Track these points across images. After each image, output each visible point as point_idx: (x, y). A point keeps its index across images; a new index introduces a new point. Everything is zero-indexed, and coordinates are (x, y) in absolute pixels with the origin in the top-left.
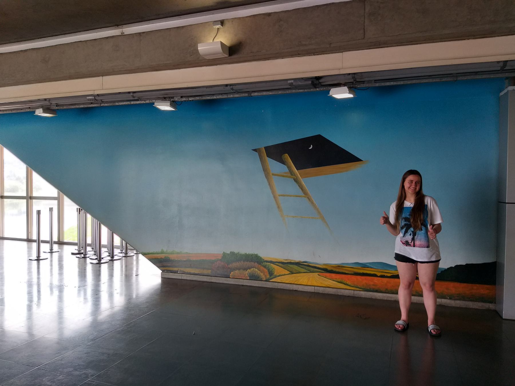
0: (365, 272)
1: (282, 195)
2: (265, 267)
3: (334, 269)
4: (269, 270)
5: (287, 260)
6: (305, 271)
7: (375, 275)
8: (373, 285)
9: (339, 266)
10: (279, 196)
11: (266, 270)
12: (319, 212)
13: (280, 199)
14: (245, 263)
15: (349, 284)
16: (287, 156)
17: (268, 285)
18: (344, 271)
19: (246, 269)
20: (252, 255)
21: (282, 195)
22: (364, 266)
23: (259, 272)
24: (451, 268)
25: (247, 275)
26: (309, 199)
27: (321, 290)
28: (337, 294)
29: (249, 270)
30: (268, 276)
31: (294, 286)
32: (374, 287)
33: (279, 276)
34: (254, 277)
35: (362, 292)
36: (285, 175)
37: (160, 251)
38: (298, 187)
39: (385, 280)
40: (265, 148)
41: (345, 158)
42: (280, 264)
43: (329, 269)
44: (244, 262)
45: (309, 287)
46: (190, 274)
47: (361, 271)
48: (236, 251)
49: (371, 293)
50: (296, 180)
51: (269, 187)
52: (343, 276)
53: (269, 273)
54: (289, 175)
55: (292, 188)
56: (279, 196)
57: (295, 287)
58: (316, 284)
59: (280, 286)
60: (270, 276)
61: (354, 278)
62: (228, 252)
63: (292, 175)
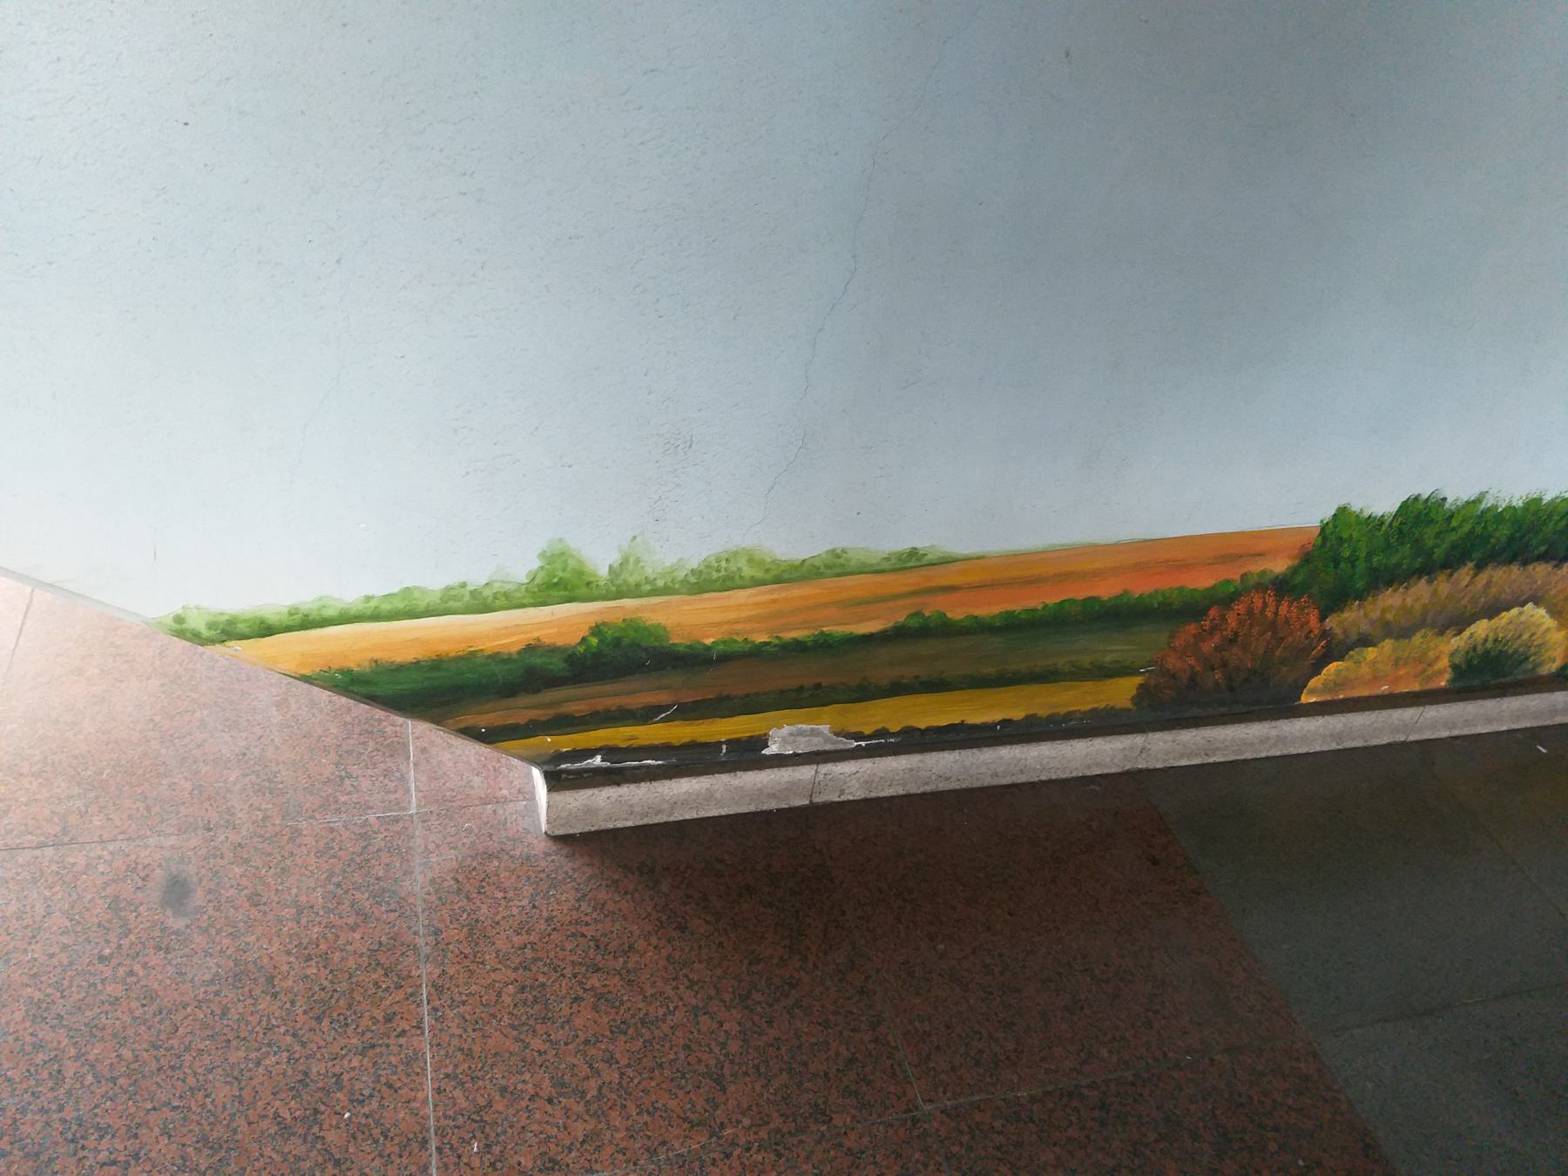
14: (1483, 578)
19: (1460, 623)
23: (1549, 622)
25: (1444, 663)
29: (1481, 628)
37: (521, 567)
48: (1457, 491)
62: (1382, 502)
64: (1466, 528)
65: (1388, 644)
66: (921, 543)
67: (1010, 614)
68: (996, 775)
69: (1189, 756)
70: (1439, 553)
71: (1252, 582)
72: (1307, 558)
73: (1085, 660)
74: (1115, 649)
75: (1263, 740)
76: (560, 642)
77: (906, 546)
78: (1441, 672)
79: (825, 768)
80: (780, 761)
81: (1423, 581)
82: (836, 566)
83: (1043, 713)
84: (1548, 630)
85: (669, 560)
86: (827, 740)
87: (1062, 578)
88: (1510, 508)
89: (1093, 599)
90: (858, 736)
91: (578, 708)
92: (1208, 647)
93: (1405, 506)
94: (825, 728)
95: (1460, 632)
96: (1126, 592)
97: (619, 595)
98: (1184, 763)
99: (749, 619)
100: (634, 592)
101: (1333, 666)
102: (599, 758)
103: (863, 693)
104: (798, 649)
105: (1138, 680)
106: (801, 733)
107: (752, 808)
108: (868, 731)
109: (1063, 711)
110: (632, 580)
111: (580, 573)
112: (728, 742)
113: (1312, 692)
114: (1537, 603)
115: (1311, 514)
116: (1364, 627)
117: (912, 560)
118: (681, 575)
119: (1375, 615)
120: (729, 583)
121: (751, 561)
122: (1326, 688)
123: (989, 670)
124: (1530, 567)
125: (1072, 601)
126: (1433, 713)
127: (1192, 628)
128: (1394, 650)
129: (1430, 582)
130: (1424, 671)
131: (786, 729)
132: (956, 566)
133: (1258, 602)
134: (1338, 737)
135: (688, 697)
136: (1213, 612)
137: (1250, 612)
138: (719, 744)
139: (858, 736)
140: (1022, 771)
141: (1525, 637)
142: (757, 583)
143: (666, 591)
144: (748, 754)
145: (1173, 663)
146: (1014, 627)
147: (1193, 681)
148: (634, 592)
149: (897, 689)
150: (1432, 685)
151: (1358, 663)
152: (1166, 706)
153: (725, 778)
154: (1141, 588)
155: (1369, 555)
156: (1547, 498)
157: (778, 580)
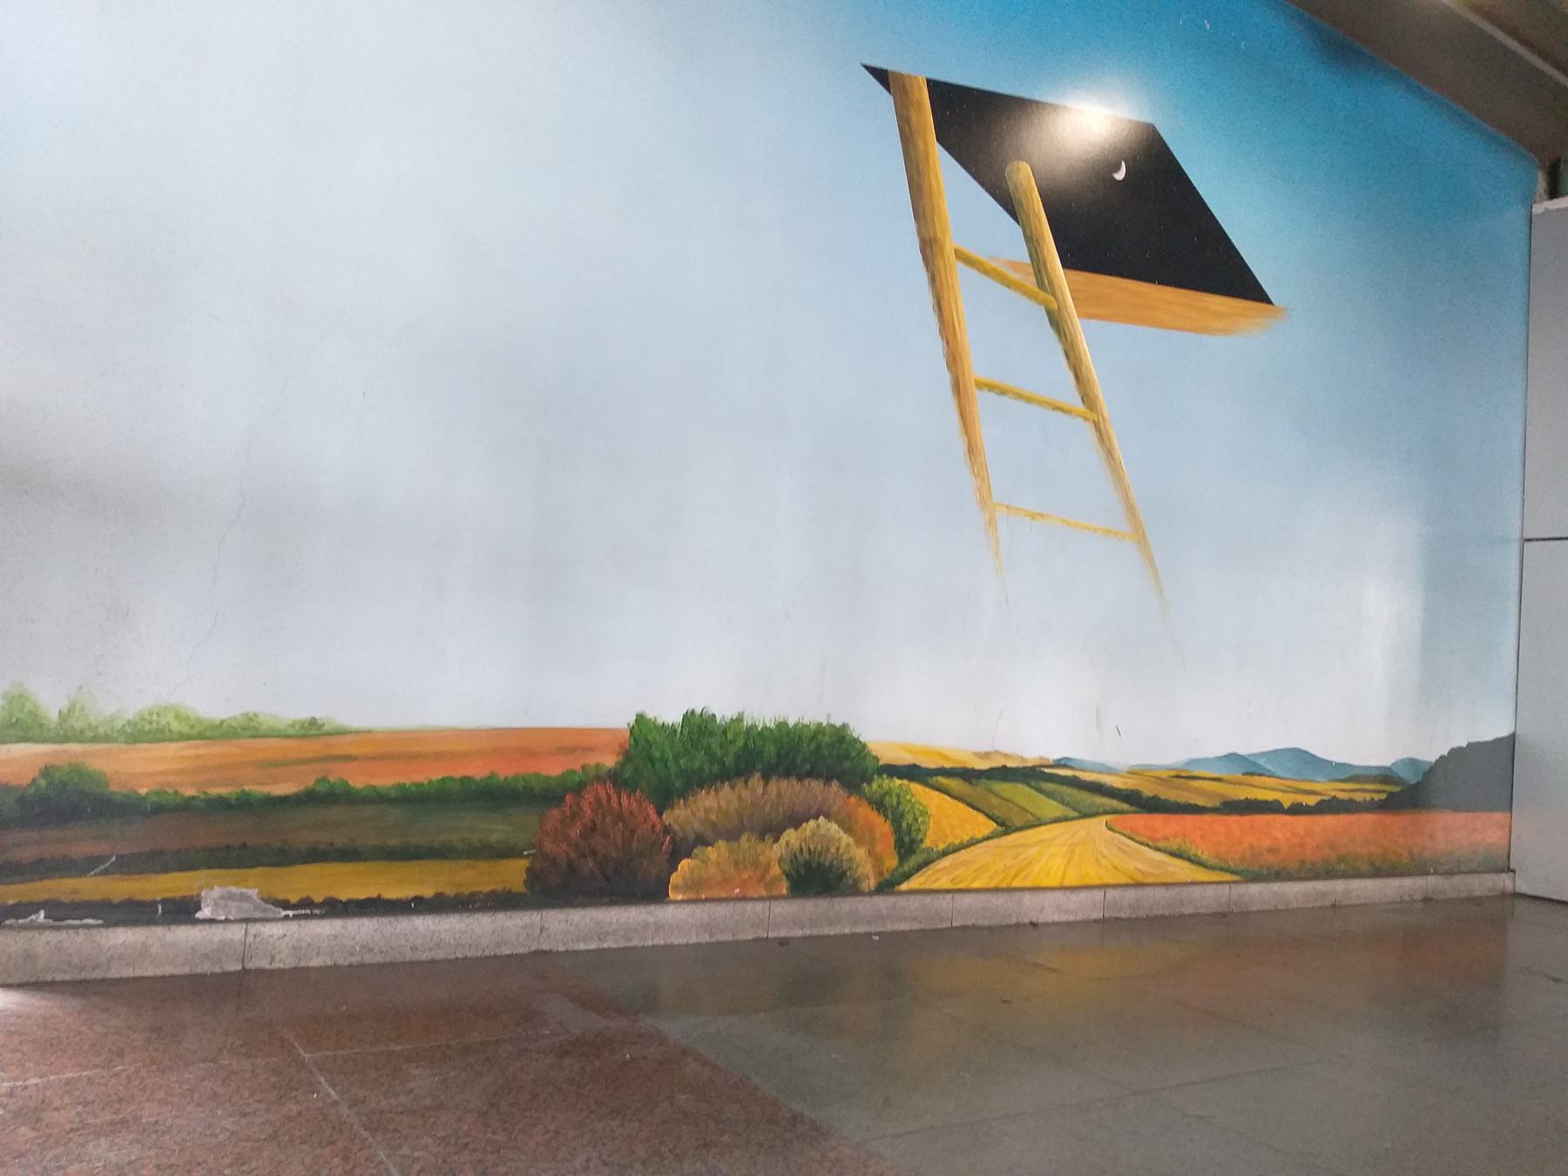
1: (991, 387)
2: (879, 805)
4: (897, 820)
8: (1270, 851)
9: (1181, 776)
10: (981, 385)
11: (883, 827)
12: (1131, 509)
13: (983, 402)
14: (773, 786)
15: (1204, 856)
19: (772, 830)
20: (820, 730)
21: (991, 387)
22: (1250, 767)
23: (846, 839)
24: (1442, 757)
25: (776, 870)
29: (790, 836)
30: (892, 862)
32: (1270, 858)
33: (945, 853)
34: (816, 877)
35: (1254, 889)
36: (1014, 275)
39: (1301, 821)
40: (935, 87)
41: (1228, 276)
42: (954, 784)
43: (1148, 791)
44: (766, 778)
45: (1083, 896)
46: (334, 908)
48: (723, 711)
49: (1276, 887)
50: (1057, 322)
52: (1190, 820)
53: (900, 844)
54: (1030, 282)
56: (981, 385)
58: (1094, 875)
59: (965, 910)
60: (903, 858)
63: (1041, 285)
64: (740, 743)
65: (721, 843)
66: (319, 715)
67: (400, 787)
68: (414, 949)
69: (586, 939)
71: (592, 774)
72: (628, 756)
73: (475, 838)
74: (496, 829)
75: (646, 926)
76: (14, 782)
77: (304, 714)
78: (775, 880)
79: (254, 929)
80: (211, 921)
82: (247, 729)
83: (450, 891)
84: (848, 845)
85: (109, 710)
86: (256, 908)
87: (439, 756)
88: (765, 728)
89: (466, 779)
90: (286, 905)
91: (27, 854)
92: (575, 832)
93: (689, 717)
94: (253, 893)
95: (776, 840)
96: (493, 775)
97: (65, 739)
98: (582, 946)
99: (178, 772)
100: (78, 737)
101: (685, 864)
102: (42, 914)
103: (285, 857)
104: (221, 806)
106: (231, 897)
107: (187, 970)
108: (294, 899)
109: (466, 891)
110: (79, 725)
111: (34, 715)
112: (164, 902)
113: (676, 888)
114: (827, 816)
115: (620, 719)
116: (697, 826)
117: (311, 730)
118: (119, 724)
119: (701, 814)
120: (159, 735)
121: (178, 716)
123: (394, 842)
124: (806, 782)
125: (451, 778)
127: (555, 813)
128: (730, 851)
129: (733, 787)
130: (763, 877)
131: (217, 891)
132: (349, 738)
133: (603, 795)
134: (708, 928)
135: (125, 849)
136: (568, 798)
137: (598, 800)
138: (154, 903)
140: (438, 946)
141: (833, 850)
142: (183, 737)
143: (107, 739)
144: (183, 911)
145: (549, 846)
146: (411, 799)
147: (572, 869)
148: (78, 737)
149: (316, 855)
150: (775, 893)
151: (704, 862)
152: (554, 886)
153: (159, 931)
154: (505, 772)
155: (676, 758)
156: (791, 723)
157: (201, 736)
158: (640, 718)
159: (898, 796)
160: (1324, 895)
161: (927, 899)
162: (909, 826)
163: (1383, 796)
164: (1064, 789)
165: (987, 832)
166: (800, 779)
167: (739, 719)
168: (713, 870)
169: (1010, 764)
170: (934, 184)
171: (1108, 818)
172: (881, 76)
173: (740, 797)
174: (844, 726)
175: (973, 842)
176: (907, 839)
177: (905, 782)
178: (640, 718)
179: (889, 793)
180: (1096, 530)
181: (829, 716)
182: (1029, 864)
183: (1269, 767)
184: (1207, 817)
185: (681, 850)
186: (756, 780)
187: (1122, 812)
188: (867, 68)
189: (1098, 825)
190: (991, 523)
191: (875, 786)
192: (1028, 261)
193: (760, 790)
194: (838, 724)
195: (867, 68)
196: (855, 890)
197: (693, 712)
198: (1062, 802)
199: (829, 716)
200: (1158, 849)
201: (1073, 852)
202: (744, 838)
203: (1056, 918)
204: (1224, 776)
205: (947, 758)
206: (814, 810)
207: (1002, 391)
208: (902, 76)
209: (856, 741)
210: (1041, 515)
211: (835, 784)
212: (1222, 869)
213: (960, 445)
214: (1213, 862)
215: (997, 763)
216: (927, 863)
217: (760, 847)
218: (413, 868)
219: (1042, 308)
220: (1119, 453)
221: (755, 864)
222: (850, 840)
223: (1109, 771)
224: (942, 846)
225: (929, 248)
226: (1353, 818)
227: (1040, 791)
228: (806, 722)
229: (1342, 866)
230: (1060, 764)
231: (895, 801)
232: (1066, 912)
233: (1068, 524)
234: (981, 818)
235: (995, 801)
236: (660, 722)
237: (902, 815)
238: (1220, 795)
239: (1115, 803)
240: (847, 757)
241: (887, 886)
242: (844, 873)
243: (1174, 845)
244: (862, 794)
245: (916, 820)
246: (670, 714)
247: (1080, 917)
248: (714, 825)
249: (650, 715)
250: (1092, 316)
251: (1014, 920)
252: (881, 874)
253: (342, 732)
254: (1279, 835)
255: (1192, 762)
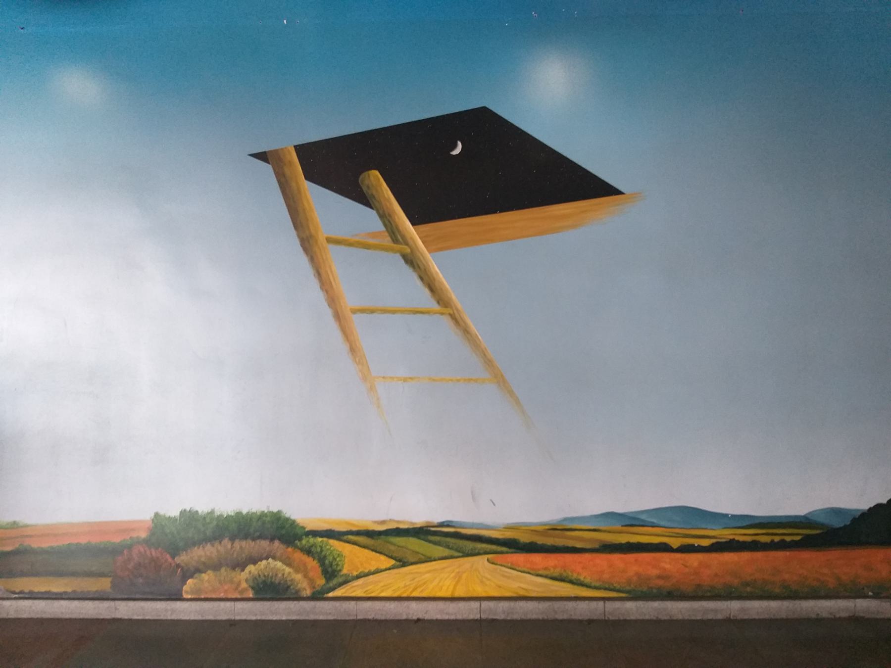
0: (634, 539)
1: (363, 311)
2: (308, 552)
3: (540, 540)
4: (322, 560)
5: (383, 522)
6: (447, 552)
7: (664, 548)
8: (659, 577)
9: (554, 529)
10: (354, 311)
11: (312, 563)
12: (489, 363)
13: (358, 322)
14: (237, 544)
15: (588, 580)
16: (375, 180)
17: (323, 611)
18: (570, 543)
19: (240, 565)
20: (263, 515)
21: (363, 311)
22: (632, 521)
23: (288, 570)
25: (244, 585)
26: (456, 319)
27: (500, 611)
28: (551, 616)
29: (251, 568)
30: (321, 582)
31: (414, 605)
32: (661, 583)
33: (358, 577)
34: (270, 590)
35: (630, 605)
36: (371, 241)
38: (419, 282)
39: (694, 559)
40: (299, 149)
43: (524, 538)
44: (232, 539)
45: (462, 605)
46: (33, 596)
47: (623, 539)
48: (202, 507)
49: (656, 604)
50: (411, 260)
51: (314, 283)
52: (569, 557)
54: (387, 241)
55: (397, 284)
56: (354, 311)
57: (415, 610)
58: (480, 591)
61: (602, 561)
62: (174, 513)
63: (395, 241)
64: (215, 523)
65: (209, 572)
67: (52, 548)
70: (208, 533)
81: (209, 544)
83: (79, 590)
84: (290, 573)
88: (228, 516)
93: (183, 513)
95: (243, 570)
101: (190, 581)
105: (110, 579)
113: (187, 592)
114: (274, 558)
115: (147, 515)
119: (196, 558)
122: (192, 592)
124: (258, 541)
126: (239, 605)
129: (213, 545)
130: (236, 589)
133: (142, 550)
137: (140, 552)
139: (14, 593)
141: (280, 575)
150: (245, 596)
154: (95, 540)
158: (157, 515)
159: (321, 547)
160: (716, 611)
161: (337, 604)
162: (331, 565)
163: (799, 538)
164: (448, 539)
165: (388, 566)
166: (254, 539)
167: (212, 512)
168: (206, 585)
169: (402, 526)
170: (305, 204)
171: (486, 557)
172: (262, 156)
173: (218, 551)
174: (279, 512)
175: (377, 571)
176: (330, 570)
177: (325, 539)
178: (157, 515)
179: (314, 545)
180: (458, 381)
181: (268, 507)
182: (424, 583)
183: (655, 521)
184: (587, 556)
185: (188, 573)
186: (226, 542)
187: (502, 553)
188: (252, 155)
189: (481, 561)
190: (372, 389)
191: (304, 542)
192: (383, 228)
193: (229, 546)
194: (275, 510)
195: (252, 155)
196: (298, 598)
197: (185, 510)
198: (448, 547)
199: (268, 507)
200: (538, 575)
201: (460, 577)
202: (223, 570)
203: (439, 617)
204: (601, 528)
205: (353, 525)
206: (264, 556)
207: (372, 311)
208: (276, 151)
209: (288, 519)
210: (411, 378)
211: (277, 543)
212: (606, 589)
213: (343, 347)
214: (597, 584)
215: (393, 526)
216: (346, 582)
217: (233, 574)
218: (65, 580)
219: (398, 257)
220: (473, 328)
221: (231, 582)
222: (291, 570)
223: (488, 528)
224: (355, 574)
225: (308, 243)
226: (759, 555)
227: (430, 542)
228: (254, 510)
229: (749, 589)
230: (442, 525)
231: (319, 549)
232: (447, 614)
233: (434, 380)
234: (383, 557)
235: (392, 548)
236: (167, 515)
237: (325, 557)
238: (600, 541)
239: (494, 547)
240: (283, 528)
241: (318, 596)
242: (289, 587)
243: (556, 572)
244: (296, 547)
245: (334, 559)
246: (173, 511)
247: (459, 617)
248: (204, 563)
249: (162, 513)
250: (441, 249)
251: (404, 617)
252: (314, 588)
253: (26, 526)
254: (667, 566)
255: (565, 519)
